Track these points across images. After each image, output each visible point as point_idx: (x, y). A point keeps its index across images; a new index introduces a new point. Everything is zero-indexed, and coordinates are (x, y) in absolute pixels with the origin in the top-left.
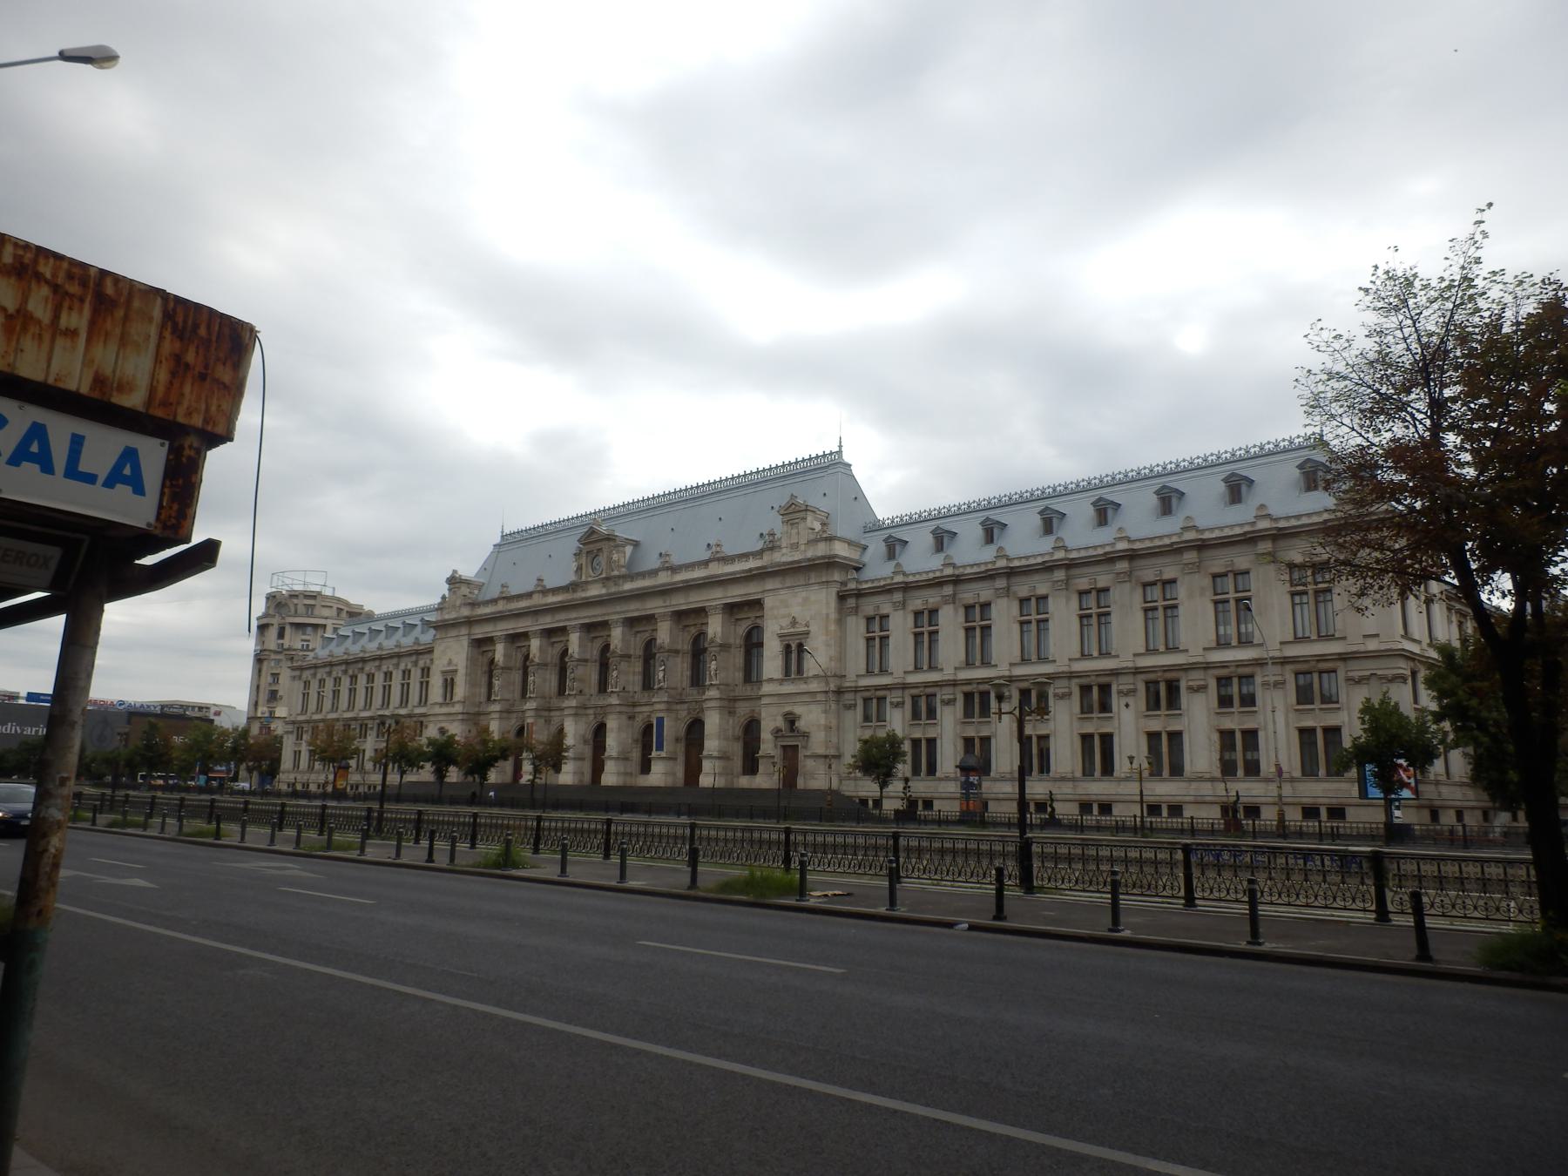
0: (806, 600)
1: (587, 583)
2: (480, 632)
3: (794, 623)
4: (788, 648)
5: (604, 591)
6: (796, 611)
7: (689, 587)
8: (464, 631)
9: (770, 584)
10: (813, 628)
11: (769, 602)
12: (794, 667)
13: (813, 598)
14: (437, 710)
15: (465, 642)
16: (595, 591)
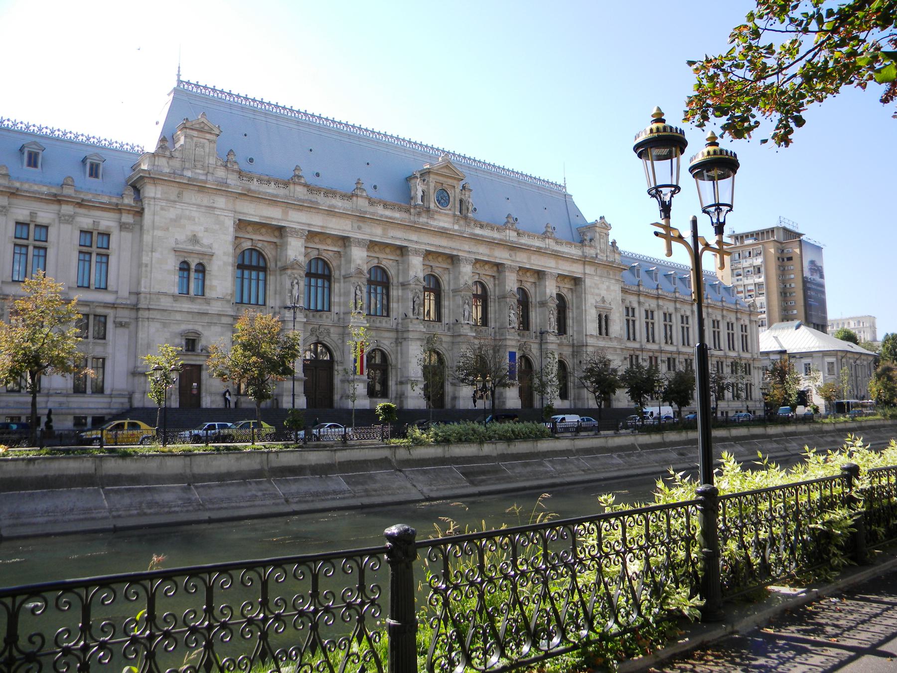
0: (608, 287)
1: (437, 212)
2: (254, 212)
3: (604, 301)
4: (600, 316)
5: (456, 227)
6: (604, 293)
7: (539, 251)
8: (221, 202)
9: (589, 270)
10: (613, 306)
11: (588, 282)
12: (604, 331)
13: (612, 288)
14: (166, 303)
15: (230, 224)
16: (443, 221)
